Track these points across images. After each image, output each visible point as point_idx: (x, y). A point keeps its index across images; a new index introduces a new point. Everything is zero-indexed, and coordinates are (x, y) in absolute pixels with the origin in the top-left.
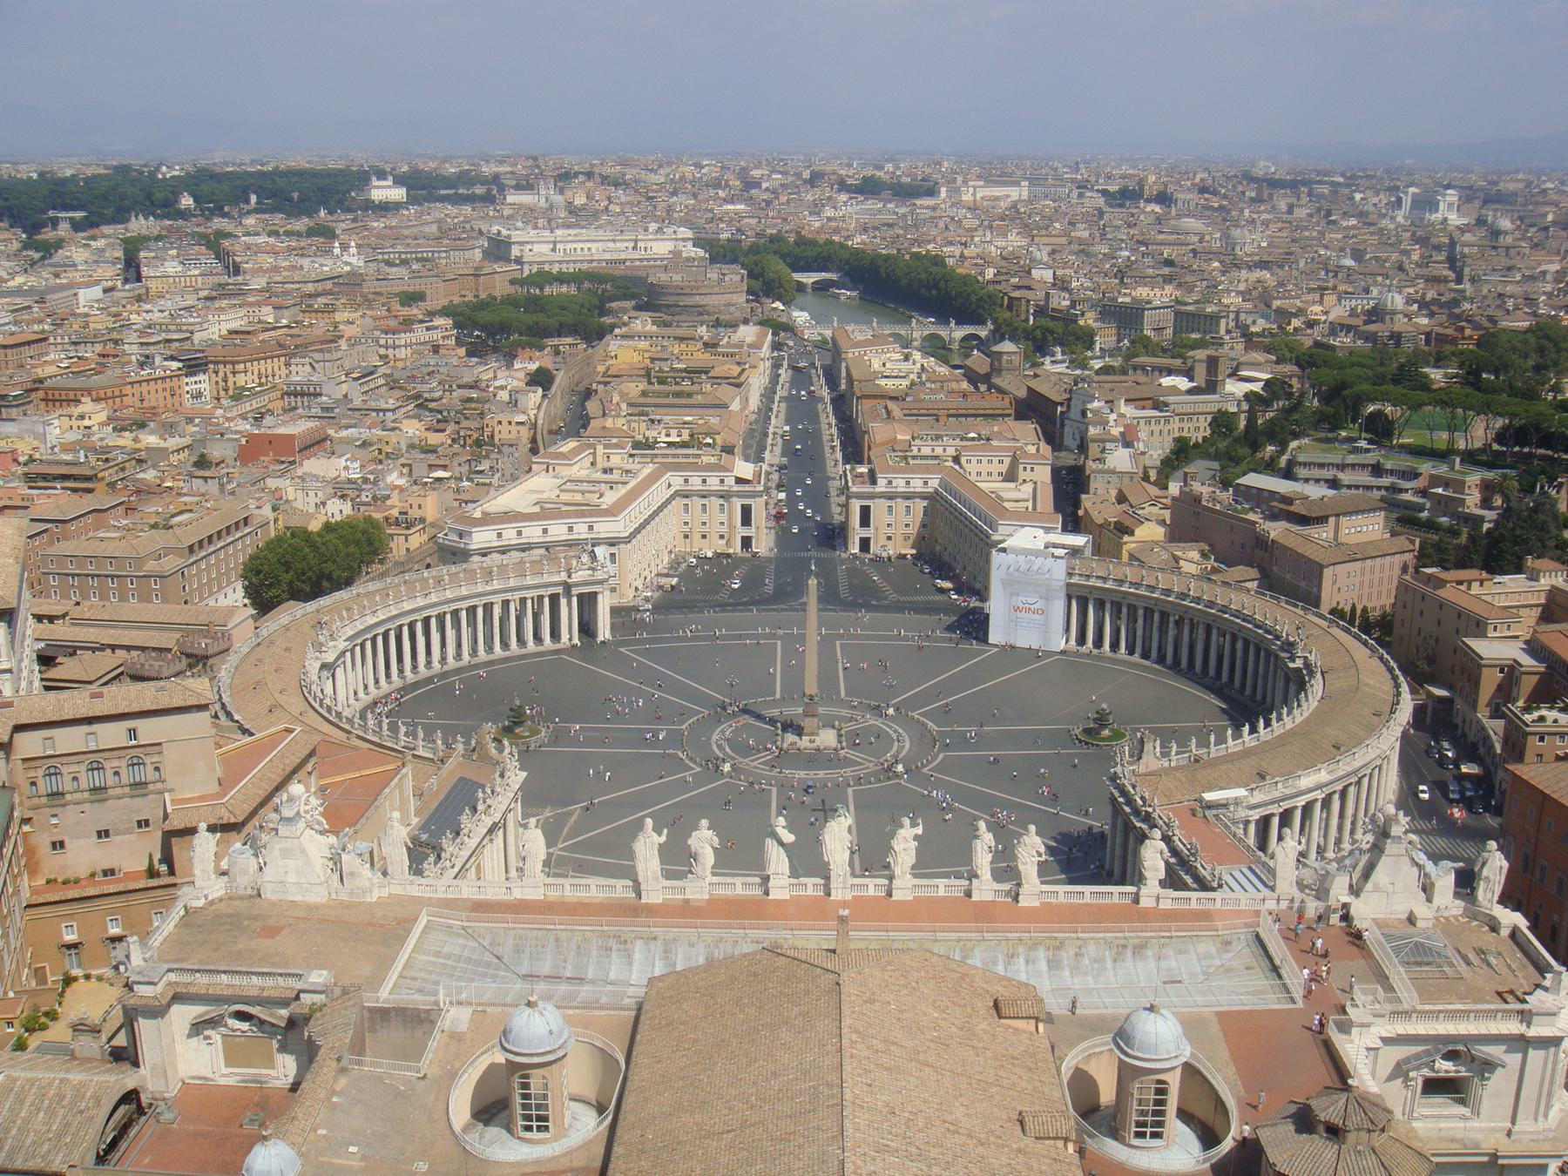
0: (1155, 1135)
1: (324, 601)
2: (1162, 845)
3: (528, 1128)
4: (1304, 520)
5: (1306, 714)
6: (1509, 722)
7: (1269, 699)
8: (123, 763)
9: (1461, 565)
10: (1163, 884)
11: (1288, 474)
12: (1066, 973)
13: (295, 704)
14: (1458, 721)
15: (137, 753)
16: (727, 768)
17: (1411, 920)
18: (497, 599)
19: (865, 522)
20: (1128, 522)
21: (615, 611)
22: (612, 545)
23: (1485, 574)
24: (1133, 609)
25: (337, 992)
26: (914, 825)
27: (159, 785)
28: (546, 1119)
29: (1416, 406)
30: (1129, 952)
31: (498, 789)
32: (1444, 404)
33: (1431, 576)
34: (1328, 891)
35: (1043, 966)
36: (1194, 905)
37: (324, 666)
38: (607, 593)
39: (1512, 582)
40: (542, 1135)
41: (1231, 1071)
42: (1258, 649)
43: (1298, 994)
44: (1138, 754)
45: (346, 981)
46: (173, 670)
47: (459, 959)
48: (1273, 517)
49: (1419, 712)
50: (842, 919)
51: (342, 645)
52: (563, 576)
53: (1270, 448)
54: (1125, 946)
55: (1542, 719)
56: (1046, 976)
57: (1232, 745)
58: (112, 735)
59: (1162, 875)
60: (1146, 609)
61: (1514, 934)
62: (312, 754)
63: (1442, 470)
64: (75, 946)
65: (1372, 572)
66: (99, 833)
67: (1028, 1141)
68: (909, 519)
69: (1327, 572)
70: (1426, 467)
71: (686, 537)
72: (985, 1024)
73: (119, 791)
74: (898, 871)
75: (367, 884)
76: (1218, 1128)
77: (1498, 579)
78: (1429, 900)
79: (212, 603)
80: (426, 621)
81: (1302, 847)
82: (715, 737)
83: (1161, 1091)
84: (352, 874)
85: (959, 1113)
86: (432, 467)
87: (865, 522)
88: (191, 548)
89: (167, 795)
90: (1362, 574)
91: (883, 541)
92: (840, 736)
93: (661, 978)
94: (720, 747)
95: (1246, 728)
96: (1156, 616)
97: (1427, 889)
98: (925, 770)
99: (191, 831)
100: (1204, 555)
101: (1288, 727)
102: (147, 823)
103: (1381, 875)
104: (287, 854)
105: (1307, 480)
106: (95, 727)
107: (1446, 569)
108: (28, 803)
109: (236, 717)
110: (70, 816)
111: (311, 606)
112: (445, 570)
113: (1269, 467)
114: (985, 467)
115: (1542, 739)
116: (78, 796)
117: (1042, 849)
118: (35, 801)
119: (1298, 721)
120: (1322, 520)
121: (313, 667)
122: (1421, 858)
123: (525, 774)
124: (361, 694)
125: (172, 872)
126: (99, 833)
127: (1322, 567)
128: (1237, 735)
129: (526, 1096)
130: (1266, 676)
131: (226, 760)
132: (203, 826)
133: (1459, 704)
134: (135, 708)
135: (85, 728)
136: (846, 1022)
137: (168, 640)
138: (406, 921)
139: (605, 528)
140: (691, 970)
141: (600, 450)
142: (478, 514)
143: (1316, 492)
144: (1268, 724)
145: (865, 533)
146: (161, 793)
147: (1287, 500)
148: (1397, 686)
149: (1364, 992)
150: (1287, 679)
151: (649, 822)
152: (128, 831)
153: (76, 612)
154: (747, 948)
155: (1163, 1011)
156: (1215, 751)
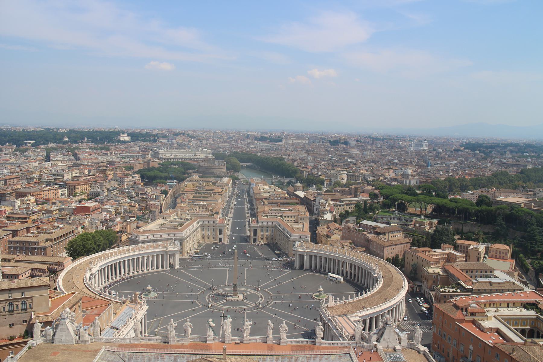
1: (93, 256)
2: (322, 327)
5: (378, 289)
6: (436, 292)
9: (424, 246)
10: (323, 339)
11: (375, 221)
13: (80, 285)
14: (422, 292)
15: (24, 301)
16: (210, 306)
17: (395, 350)
19: (255, 234)
20: (329, 234)
21: (180, 259)
22: (181, 240)
23: (430, 249)
24: (330, 259)
26: (250, 321)
27: (31, 310)
29: (410, 202)
30: (312, 359)
31: (139, 312)
32: (418, 201)
33: (414, 250)
34: (370, 340)
36: (332, 345)
37: (91, 275)
38: (178, 254)
39: (439, 251)
42: (365, 271)
44: (327, 300)
46: (45, 275)
48: (370, 233)
50: (224, 349)
51: (97, 268)
52: (165, 249)
54: (311, 357)
58: (17, 295)
59: (322, 336)
60: (334, 259)
61: (424, 354)
62: (80, 300)
63: (418, 219)
65: (398, 248)
66: (10, 325)
69: (386, 249)
70: (415, 219)
71: (203, 238)
74: (245, 335)
75: (87, 339)
77: (434, 250)
78: (400, 343)
79: (61, 255)
80: (124, 261)
81: (363, 328)
82: (207, 297)
84: (83, 336)
87: (255, 234)
88: (55, 239)
90: (396, 249)
91: (260, 240)
92: (244, 296)
94: (209, 299)
96: (337, 261)
98: (268, 306)
100: (350, 244)
101: (372, 293)
102: (26, 321)
103: (385, 336)
104: (63, 330)
105: (380, 223)
107: (419, 247)
109: (63, 289)
110: (1, 319)
111: (89, 257)
112: (130, 247)
113: (370, 219)
115: (445, 297)
116: (4, 313)
117: (287, 328)
119: (375, 291)
120: (384, 234)
121: (88, 274)
122: (397, 331)
124: (103, 283)
126: (10, 325)
127: (384, 247)
128: (357, 296)
130: (368, 279)
132: (38, 321)
133: (423, 285)
134: (25, 286)
137: (45, 267)
138: (97, 350)
139: (178, 236)
141: (179, 213)
142: (142, 231)
144: (366, 293)
145: (255, 237)
147: (374, 228)
148: (404, 281)
151: (172, 320)
153: (17, 258)
156: (350, 300)
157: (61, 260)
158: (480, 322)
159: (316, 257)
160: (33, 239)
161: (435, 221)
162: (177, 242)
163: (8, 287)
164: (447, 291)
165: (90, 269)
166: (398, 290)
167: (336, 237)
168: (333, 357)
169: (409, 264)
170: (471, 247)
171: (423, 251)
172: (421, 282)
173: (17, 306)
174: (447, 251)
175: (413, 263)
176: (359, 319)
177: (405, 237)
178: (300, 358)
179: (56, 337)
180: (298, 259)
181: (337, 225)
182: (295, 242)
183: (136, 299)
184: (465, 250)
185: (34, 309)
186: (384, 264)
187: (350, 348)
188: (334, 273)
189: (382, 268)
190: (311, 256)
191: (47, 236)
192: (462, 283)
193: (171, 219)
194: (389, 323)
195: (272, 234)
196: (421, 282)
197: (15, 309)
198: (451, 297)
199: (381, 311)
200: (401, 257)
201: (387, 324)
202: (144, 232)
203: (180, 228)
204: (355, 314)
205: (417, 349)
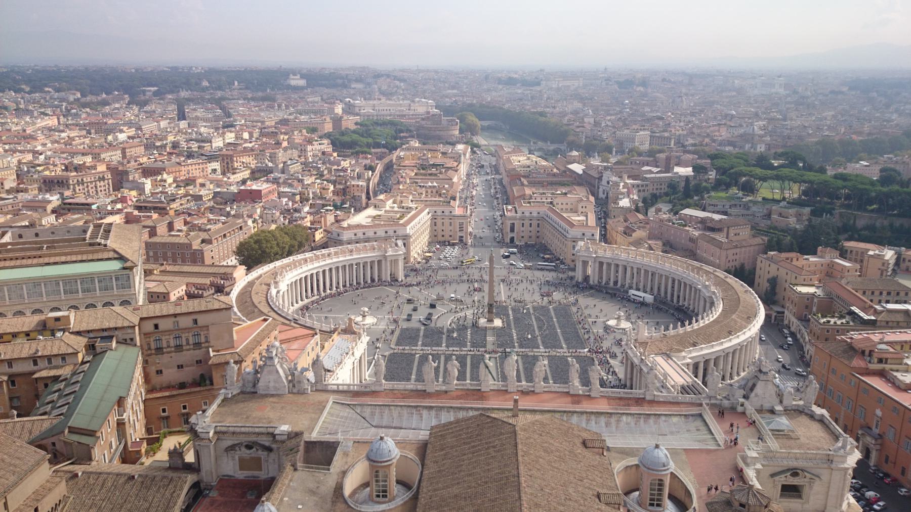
0: (658, 505)
1: (278, 263)
3: (378, 496)
4: (712, 230)
5: (715, 317)
7: (696, 311)
8: (190, 334)
11: (704, 210)
12: (614, 428)
13: (266, 309)
14: (786, 322)
17: (772, 412)
18: (354, 263)
19: (512, 230)
25: (293, 435)
27: (207, 344)
28: (386, 491)
29: (764, 179)
30: (642, 420)
32: (777, 178)
35: (603, 425)
37: (278, 292)
39: (812, 259)
40: (384, 499)
41: (692, 477)
42: (691, 287)
43: (721, 443)
45: (297, 429)
47: (346, 418)
49: (768, 317)
50: (516, 401)
53: (696, 198)
55: (829, 322)
56: (604, 429)
57: (681, 330)
64: (167, 418)
66: (178, 367)
67: (603, 507)
68: (530, 229)
72: (580, 450)
73: (188, 347)
74: (537, 380)
76: (687, 501)
78: (781, 402)
79: (225, 264)
80: (324, 271)
83: (661, 484)
85: (571, 490)
86: (324, 206)
87: (512, 230)
89: (211, 350)
93: (436, 427)
95: (687, 323)
96: (643, 272)
97: (780, 396)
99: (227, 363)
101: (707, 322)
102: (201, 361)
104: (270, 372)
106: (178, 319)
108: (146, 353)
110: (165, 359)
111: (271, 266)
114: (564, 207)
115: (828, 331)
116: (169, 350)
118: (149, 352)
119: (712, 320)
120: (720, 230)
123: (368, 338)
125: (212, 384)
126: (178, 367)
128: (683, 325)
129: (377, 481)
130: (694, 299)
131: (237, 332)
132: (232, 361)
134: (197, 310)
135: (173, 319)
136: (520, 446)
137: (207, 281)
140: (451, 423)
143: (717, 217)
144: (697, 321)
145: (512, 235)
146: (208, 348)
149: (753, 443)
150: (705, 301)
152: (192, 365)
153: (163, 268)
154: (471, 413)
155: (661, 447)
157: (228, 270)
158: (895, 374)
159: (609, 265)
160: (183, 240)
161: (807, 210)
162: (400, 243)
163: (171, 312)
164: (832, 323)
165: (276, 283)
166: (750, 318)
167: (639, 234)
168: (675, 420)
169: (762, 278)
170: (871, 253)
171: (787, 259)
172: (783, 307)
173: (187, 340)
174: (826, 260)
175: (771, 276)
176: (689, 361)
177: (754, 236)
178: (624, 418)
179: (260, 384)
180: (581, 267)
181: (641, 216)
182: (575, 241)
183: (350, 325)
184: (859, 258)
185: (212, 344)
186: (723, 277)
187: (701, 405)
188: (638, 290)
189: (720, 283)
190: (601, 264)
191: (204, 235)
192: (857, 311)
193: (388, 208)
194: (764, 370)
195: (538, 229)
196: (783, 307)
197: (184, 343)
198: (838, 331)
199: (723, 350)
200: (747, 267)
201: (760, 371)
202: (350, 227)
203: (401, 222)
204: (683, 354)
205: (809, 412)
